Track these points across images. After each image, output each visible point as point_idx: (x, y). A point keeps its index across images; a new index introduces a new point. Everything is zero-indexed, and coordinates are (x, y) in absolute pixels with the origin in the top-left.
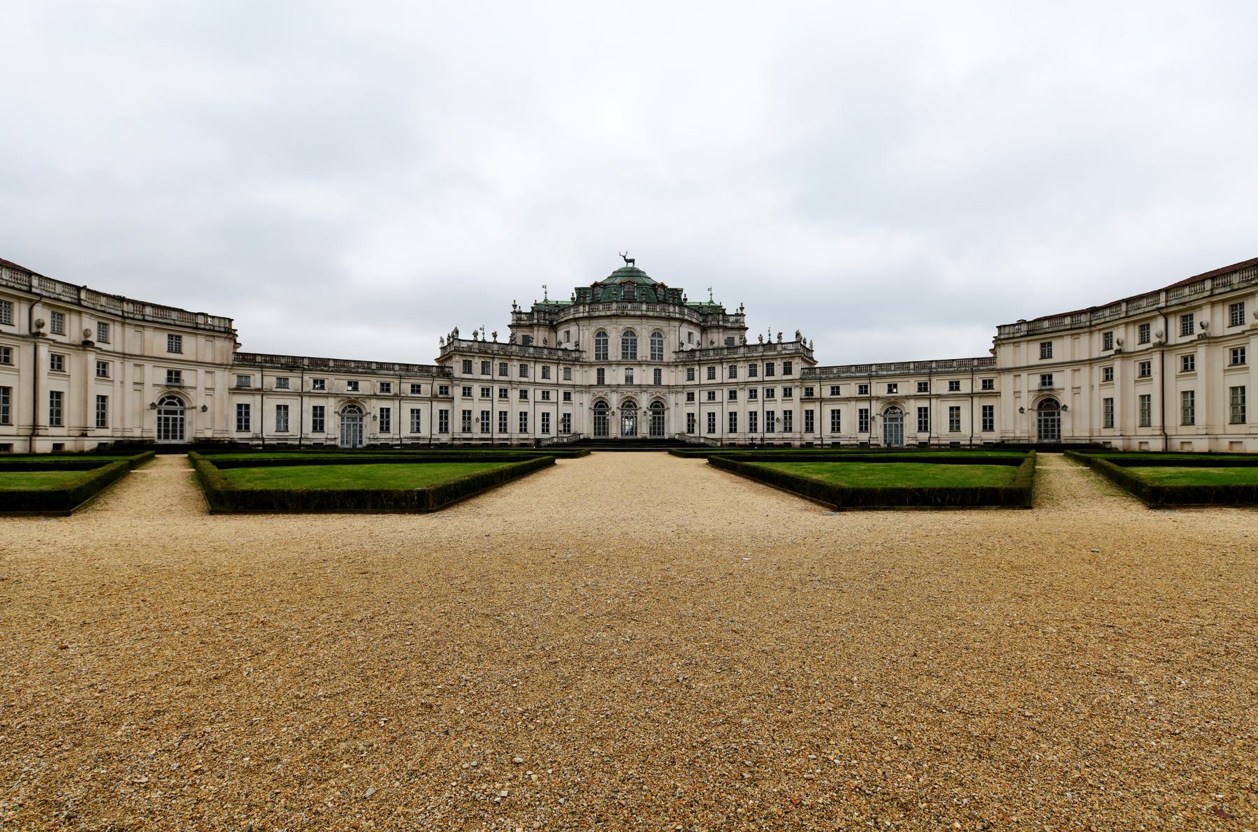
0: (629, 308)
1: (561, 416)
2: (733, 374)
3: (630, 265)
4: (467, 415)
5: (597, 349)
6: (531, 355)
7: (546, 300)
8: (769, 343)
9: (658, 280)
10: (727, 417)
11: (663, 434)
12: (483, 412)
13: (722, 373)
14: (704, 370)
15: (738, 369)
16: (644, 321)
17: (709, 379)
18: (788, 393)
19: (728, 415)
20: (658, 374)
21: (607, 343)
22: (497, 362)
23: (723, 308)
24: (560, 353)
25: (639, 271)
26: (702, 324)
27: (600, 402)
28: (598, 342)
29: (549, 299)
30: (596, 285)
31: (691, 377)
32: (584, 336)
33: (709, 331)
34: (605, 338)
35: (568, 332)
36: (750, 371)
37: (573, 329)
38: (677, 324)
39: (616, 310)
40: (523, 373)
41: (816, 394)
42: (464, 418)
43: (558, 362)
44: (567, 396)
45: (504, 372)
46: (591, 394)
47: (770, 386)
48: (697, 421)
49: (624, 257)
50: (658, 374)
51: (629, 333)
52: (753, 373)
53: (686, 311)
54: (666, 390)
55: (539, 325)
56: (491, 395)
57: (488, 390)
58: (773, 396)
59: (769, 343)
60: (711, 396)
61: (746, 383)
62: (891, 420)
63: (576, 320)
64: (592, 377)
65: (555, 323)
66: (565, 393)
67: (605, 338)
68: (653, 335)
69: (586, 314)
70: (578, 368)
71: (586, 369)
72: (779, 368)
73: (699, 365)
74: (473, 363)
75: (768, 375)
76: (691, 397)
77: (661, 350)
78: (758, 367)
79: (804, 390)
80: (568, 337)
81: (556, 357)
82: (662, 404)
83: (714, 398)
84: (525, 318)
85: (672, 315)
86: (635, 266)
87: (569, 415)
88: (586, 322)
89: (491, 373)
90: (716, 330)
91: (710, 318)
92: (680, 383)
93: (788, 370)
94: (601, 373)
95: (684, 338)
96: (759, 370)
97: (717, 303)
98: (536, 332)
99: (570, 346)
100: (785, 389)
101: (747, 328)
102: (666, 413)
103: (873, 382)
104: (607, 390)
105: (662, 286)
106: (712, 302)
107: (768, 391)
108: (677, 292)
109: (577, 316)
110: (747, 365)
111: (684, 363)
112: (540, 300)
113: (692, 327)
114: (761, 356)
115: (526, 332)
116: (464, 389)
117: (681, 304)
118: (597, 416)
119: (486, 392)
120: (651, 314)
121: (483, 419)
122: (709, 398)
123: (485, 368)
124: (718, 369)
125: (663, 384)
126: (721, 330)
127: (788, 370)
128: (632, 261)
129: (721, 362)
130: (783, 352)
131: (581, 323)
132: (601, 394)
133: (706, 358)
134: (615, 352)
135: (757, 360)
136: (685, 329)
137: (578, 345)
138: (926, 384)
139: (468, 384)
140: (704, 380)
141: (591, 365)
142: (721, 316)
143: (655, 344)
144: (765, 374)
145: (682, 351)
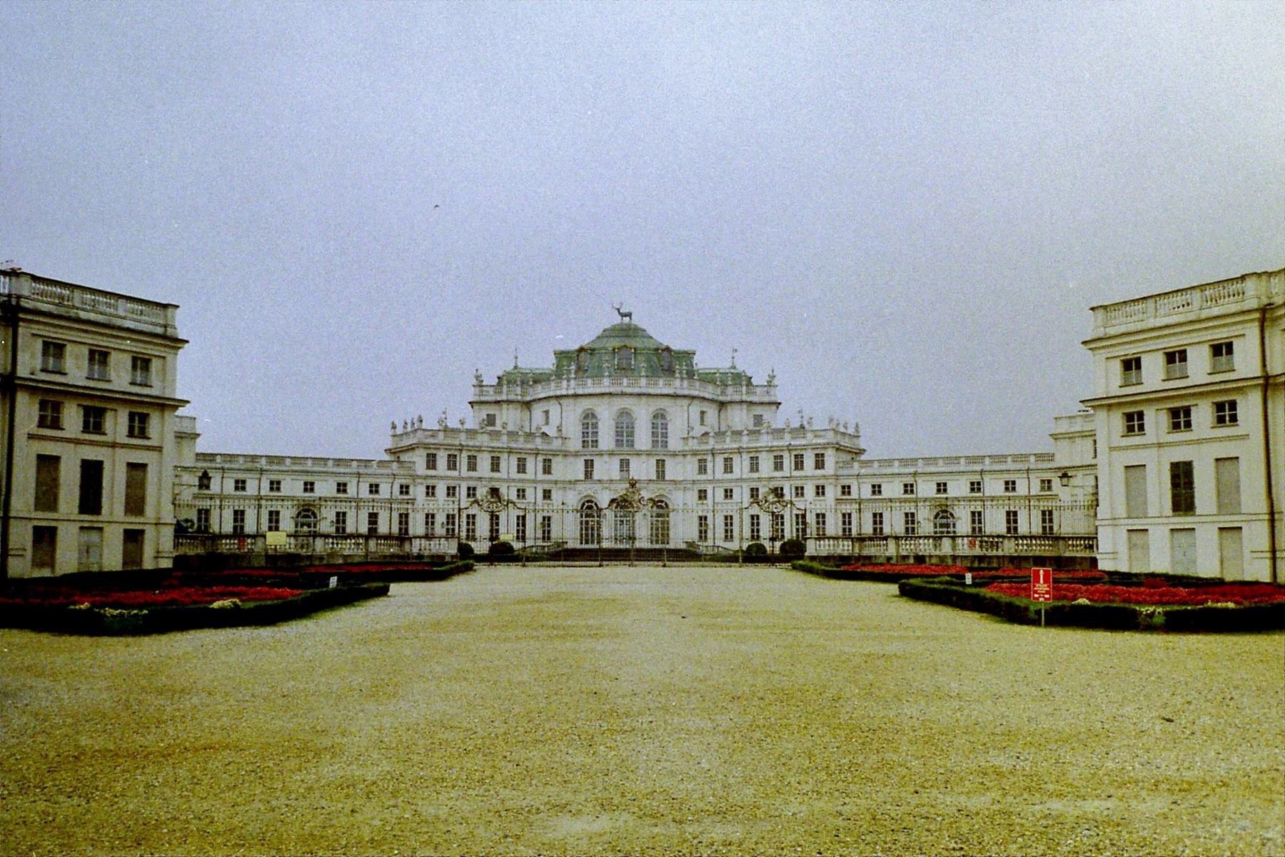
0: (625, 384)
1: (540, 520)
2: (754, 467)
3: (626, 320)
4: (430, 518)
5: (585, 434)
6: (505, 446)
7: (516, 367)
8: (802, 427)
9: (665, 343)
10: (747, 521)
11: (668, 543)
12: (448, 516)
13: (741, 466)
14: (720, 460)
15: (760, 461)
16: (644, 399)
17: (726, 472)
18: (820, 491)
19: (750, 518)
20: (660, 464)
21: (596, 428)
22: (465, 454)
23: (749, 374)
24: (538, 440)
25: (637, 329)
26: (721, 398)
27: (588, 501)
28: (586, 426)
29: (519, 365)
30: (581, 350)
31: (702, 469)
32: (567, 419)
33: (729, 407)
34: (594, 421)
35: (547, 412)
36: (776, 463)
37: (554, 408)
38: (686, 402)
39: (609, 386)
40: (495, 466)
41: (854, 495)
42: (427, 523)
43: (537, 453)
44: (547, 495)
45: (472, 466)
46: (576, 493)
47: (799, 483)
48: (711, 526)
49: (618, 310)
50: (660, 464)
51: (624, 413)
52: (778, 466)
53: (697, 384)
54: (671, 487)
55: (509, 402)
56: (457, 494)
57: (454, 488)
58: (802, 495)
59: (802, 427)
60: (728, 494)
61: (771, 479)
62: (942, 525)
63: (557, 397)
64: (576, 469)
65: (528, 398)
66: (545, 491)
67: (594, 421)
68: (655, 417)
69: (571, 392)
70: (559, 459)
71: (571, 459)
72: (809, 461)
73: (713, 454)
74: (438, 457)
75: (796, 469)
76: (702, 495)
77: (665, 435)
78: (784, 460)
79: (839, 489)
80: (547, 418)
81: (533, 447)
82: (666, 504)
83: (731, 496)
84: (492, 393)
85: (680, 392)
86: (633, 322)
87: (549, 518)
88: (571, 401)
89: (458, 467)
90: (737, 407)
91: (730, 390)
92: (690, 478)
93: (820, 464)
94: (589, 465)
95: (695, 415)
96: (786, 462)
97: (740, 368)
98: (504, 411)
99: (551, 431)
100: (818, 487)
101: (780, 404)
102: (671, 515)
103: (919, 480)
104: (599, 486)
105: (668, 349)
106: (734, 368)
107: (797, 488)
108: (688, 356)
109: (558, 393)
110: (771, 456)
111: (694, 453)
112: (510, 368)
113: (706, 403)
114: (787, 446)
115: (492, 410)
116: (428, 487)
117: (691, 374)
118: (584, 519)
119: (451, 491)
120: (652, 391)
121: (448, 523)
122: (726, 497)
123: (452, 464)
124: (736, 459)
125: (667, 478)
126: (745, 406)
127: (820, 464)
128: (629, 315)
129: (739, 451)
130: (814, 442)
131: (563, 401)
132: (590, 492)
133: (720, 447)
134: (606, 439)
135: (783, 450)
136: (696, 409)
137: (560, 430)
138: (979, 483)
139: (430, 482)
140: (720, 474)
141: (576, 454)
142: (744, 388)
143: (657, 428)
144: (793, 468)
145: (693, 438)
